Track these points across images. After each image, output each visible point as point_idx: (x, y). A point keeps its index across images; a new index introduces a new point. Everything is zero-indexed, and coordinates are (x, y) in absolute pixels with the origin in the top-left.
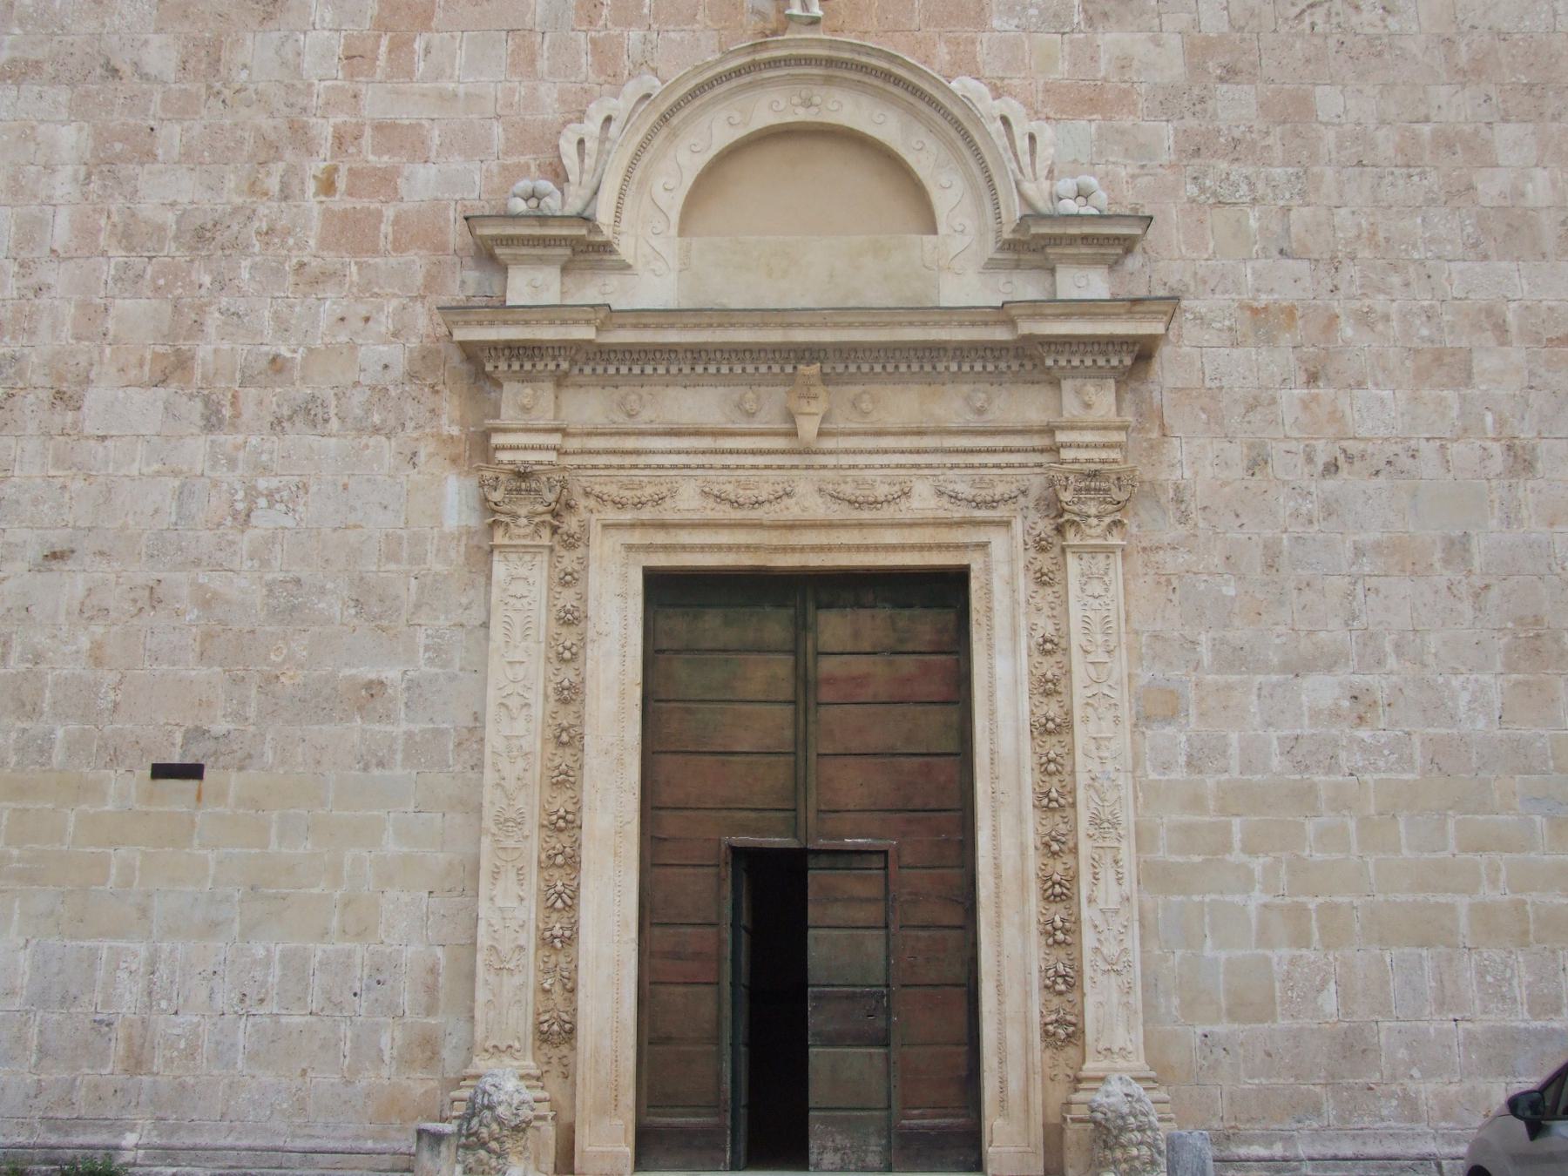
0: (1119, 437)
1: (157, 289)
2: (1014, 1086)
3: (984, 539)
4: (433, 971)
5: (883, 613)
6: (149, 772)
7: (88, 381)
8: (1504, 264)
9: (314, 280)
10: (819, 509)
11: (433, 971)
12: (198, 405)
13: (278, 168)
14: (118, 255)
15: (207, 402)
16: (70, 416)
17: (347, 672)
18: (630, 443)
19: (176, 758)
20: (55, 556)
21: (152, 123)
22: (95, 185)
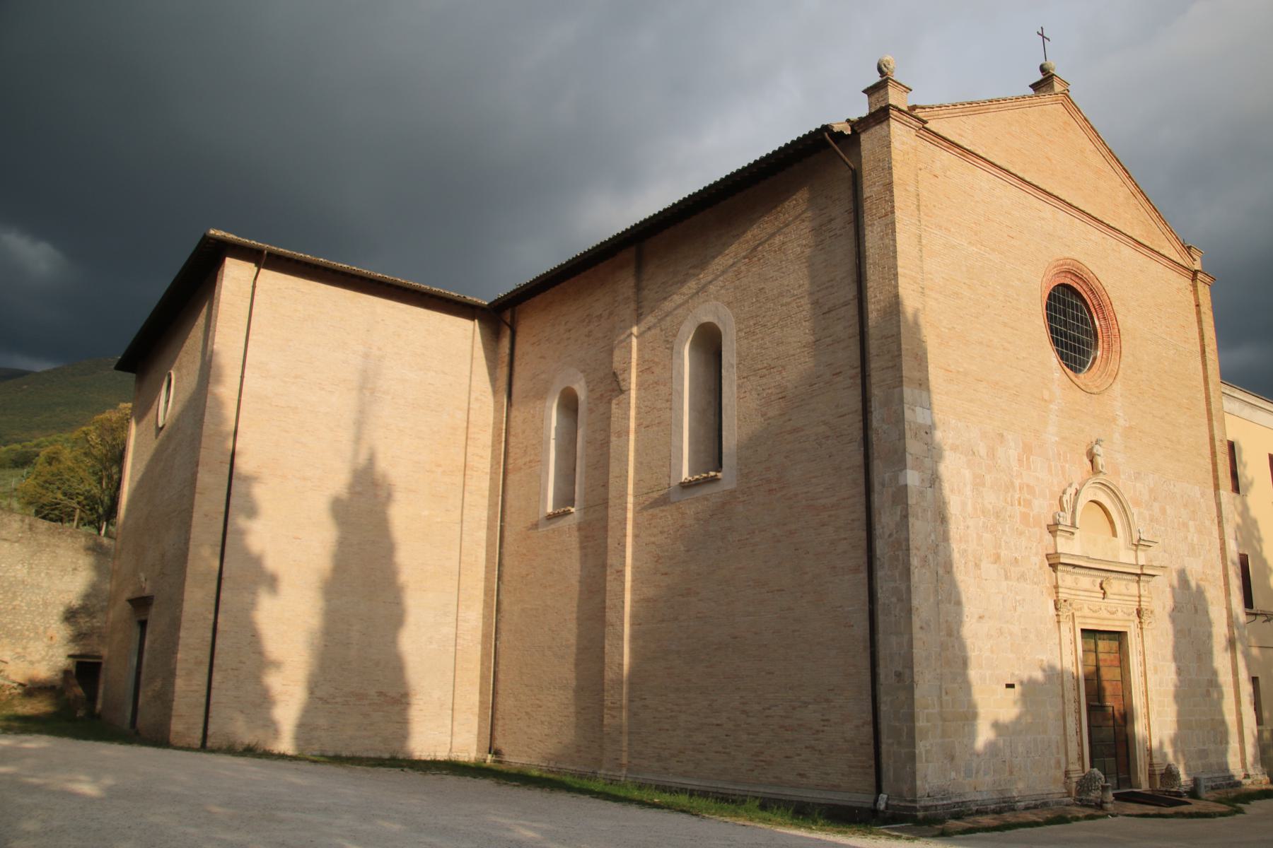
0: (1150, 600)
1: (991, 531)
2: (1143, 767)
3: (1128, 625)
4: (1057, 742)
5: (1108, 641)
6: (1005, 686)
7: (981, 560)
8: (1192, 559)
9: (1021, 534)
10: (1104, 614)
11: (1057, 742)
12: (1003, 571)
13: (1010, 495)
14: (982, 519)
15: (1004, 569)
16: (979, 571)
17: (1037, 656)
18: (1073, 592)
19: (1009, 683)
20: (981, 617)
21: (984, 473)
22: (975, 493)
